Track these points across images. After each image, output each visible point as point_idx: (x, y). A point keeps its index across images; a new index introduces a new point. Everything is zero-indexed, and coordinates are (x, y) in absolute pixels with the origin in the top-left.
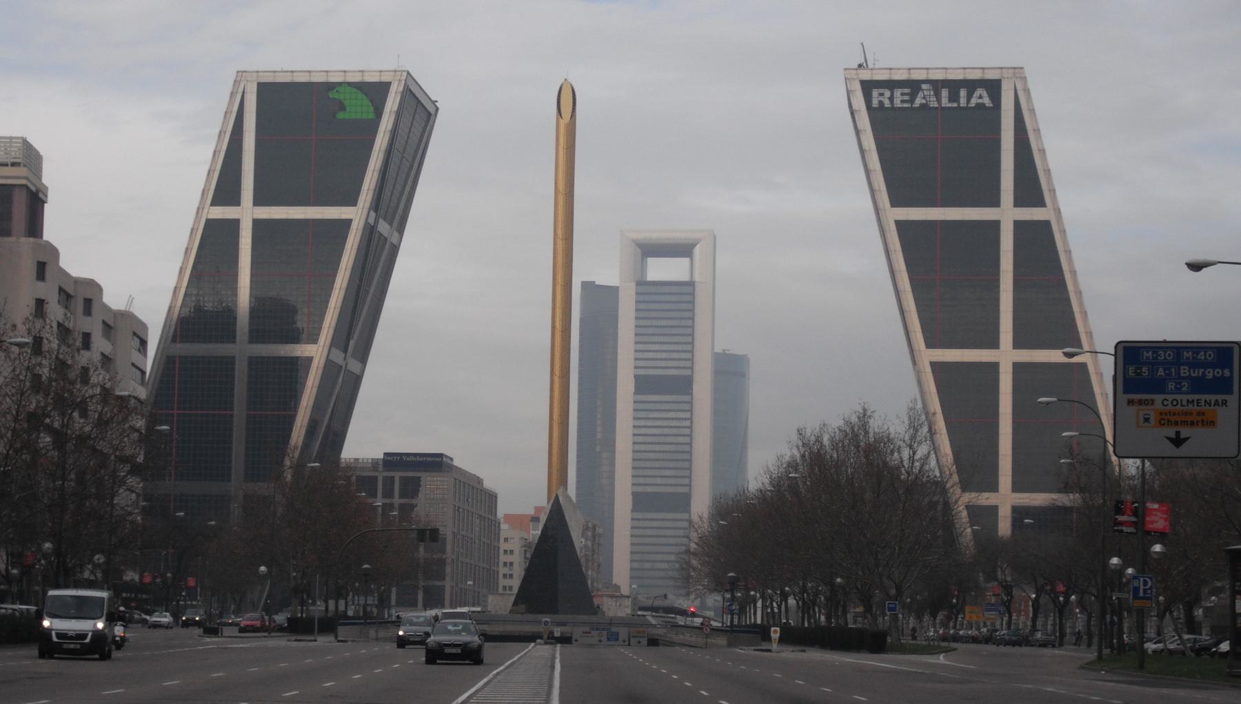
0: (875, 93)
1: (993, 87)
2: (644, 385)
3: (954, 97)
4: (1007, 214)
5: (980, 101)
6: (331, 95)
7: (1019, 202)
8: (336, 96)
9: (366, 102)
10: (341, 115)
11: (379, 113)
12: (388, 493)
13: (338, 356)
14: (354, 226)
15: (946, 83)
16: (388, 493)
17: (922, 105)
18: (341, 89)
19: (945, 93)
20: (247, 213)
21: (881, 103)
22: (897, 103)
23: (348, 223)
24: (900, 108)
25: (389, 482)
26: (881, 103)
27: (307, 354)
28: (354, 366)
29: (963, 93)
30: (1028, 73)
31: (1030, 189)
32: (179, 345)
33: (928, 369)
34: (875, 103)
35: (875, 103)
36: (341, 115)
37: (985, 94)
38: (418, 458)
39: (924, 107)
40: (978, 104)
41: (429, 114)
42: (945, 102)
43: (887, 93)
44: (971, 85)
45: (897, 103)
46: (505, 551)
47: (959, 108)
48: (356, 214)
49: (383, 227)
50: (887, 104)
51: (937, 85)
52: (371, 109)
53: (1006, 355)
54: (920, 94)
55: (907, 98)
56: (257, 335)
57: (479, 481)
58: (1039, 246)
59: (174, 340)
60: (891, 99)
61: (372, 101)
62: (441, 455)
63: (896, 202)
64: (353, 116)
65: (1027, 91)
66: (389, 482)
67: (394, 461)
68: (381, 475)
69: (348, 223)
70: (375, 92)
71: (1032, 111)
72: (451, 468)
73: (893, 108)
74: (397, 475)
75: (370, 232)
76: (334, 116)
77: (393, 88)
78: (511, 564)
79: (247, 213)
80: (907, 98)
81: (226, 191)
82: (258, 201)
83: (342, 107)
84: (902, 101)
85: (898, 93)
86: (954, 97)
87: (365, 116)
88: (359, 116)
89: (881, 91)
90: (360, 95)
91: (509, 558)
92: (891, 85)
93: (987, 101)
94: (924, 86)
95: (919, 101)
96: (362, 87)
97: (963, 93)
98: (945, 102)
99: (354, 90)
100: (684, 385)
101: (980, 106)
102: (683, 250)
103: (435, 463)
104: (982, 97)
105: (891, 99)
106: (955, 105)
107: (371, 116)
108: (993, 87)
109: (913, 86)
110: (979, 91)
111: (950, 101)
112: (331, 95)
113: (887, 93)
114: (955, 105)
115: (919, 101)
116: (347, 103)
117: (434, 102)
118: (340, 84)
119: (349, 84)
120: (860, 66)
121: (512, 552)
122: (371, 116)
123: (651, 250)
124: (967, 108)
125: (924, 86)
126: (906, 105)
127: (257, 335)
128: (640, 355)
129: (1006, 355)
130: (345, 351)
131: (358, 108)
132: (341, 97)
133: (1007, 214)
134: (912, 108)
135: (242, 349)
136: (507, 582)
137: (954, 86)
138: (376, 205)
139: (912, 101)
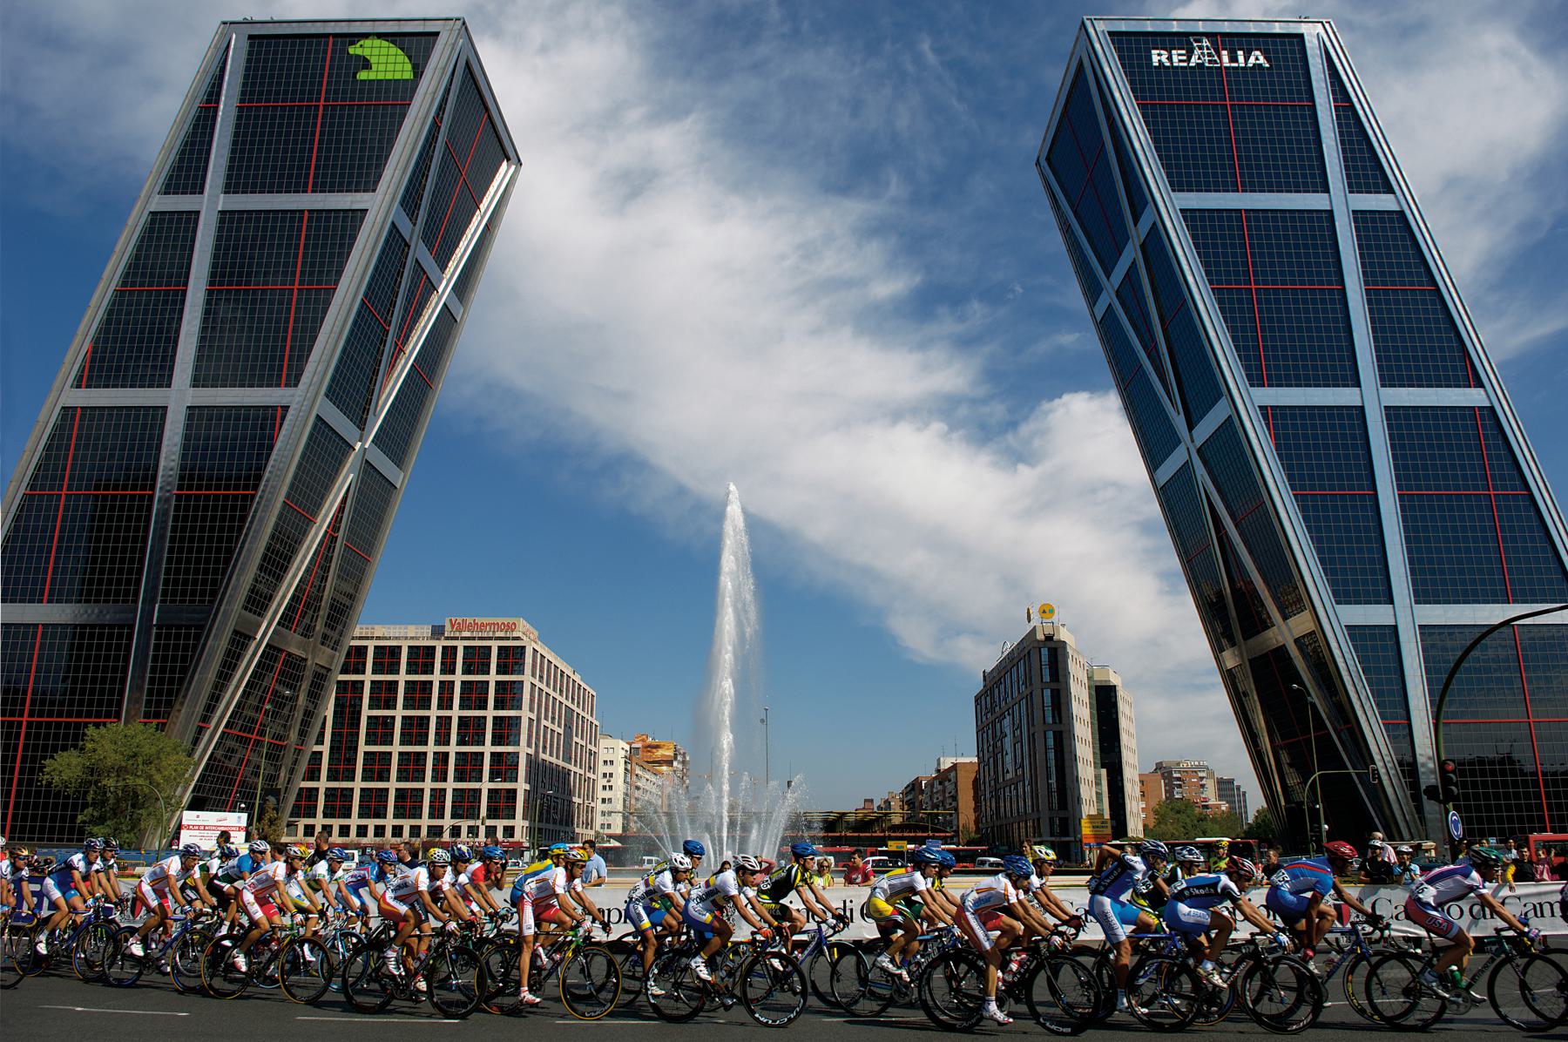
6: (351, 51)
8: (359, 52)
10: (363, 75)
11: (418, 71)
12: (449, 668)
14: (369, 218)
16: (449, 668)
18: (368, 43)
20: (212, 202)
23: (356, 217)
25: (449, 652)
31: (1368, 168)
32: (83, 392)
36: (363, 75)
49: (420, 252)
52: (409, 67)
61: (410, 58)
63: (1177, 185)
64: (381, 76)
66: (449, 652)
68: (439, 645)
69: (356, 217)
75: (395, 244)
81: (186, 172)
83: (366, 65)
87: (398, 76)
88: (389, 76)
90: (394, 50)
91: (608, 769)
95: (1194, 61)
99: (385, 44)
107: (408, 75)
112: (351, 51)
115: (1194, 61)
116: (373, 60)
118: (366, 36)
119: (380, 36)
122: (408, 75)
129: (1374, 397)
130: (361, 424)
131: (387, 64)
132: (366, 53)
133: (1341, 201)
136: (607, 794)
138: (410, 200)
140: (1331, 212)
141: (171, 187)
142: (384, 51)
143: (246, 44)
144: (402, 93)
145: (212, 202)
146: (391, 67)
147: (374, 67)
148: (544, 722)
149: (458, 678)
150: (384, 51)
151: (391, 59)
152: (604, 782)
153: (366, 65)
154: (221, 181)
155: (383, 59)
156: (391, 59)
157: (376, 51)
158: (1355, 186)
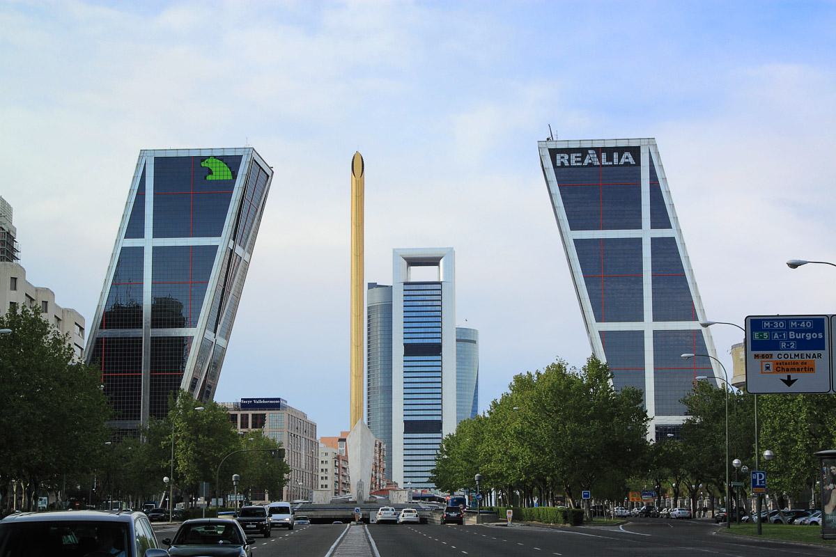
0: (558, 156)
1: (635, 151)
2: (410, 350)
3: (610, 158)
4: (646, 233)
5: (627, 160)
6: (203, 165)
7: (654, 226)
8: (206, 165)
9: (226, 168)
10: (209, 178)
11: (235, 175)
12: (244, 425)
13: (210, 335)
15: (604, 149)
16: (244, 425)
17: (589, 163)
18: (210, 160)
19: (604, 156)
20: (148, 242)
21: (562, 162)
22: (573, 163)
24: (574, 166)
25: (245, 418)
26: (562, 162)
27: (189, 335)
28: (221, 341)
29: (616, 155)
30: (658, 142)
31: (661, 217)
32: (105, 331)
33: (598, 336)
34: (559, 164)
35: (559, 164)
36: (209, 178)
37: (630, 156)
38: (264, 402)
39: (590, 165)
40: (625, 162)
41: (268, 176)
42: (604, 162)
43: (566, 157)
44: (621, 150)
45: (573, 163)
46: (322, 462)
47: (613, 165)
48: (222, 242)
50: (566, 164)
51: (599, 151)
53: (648, 326)
54: (588, 157)
55: (579, 159)
56: (156, 323)
57: (305, 416)
58: (667, 252)
59: (101, 327)
60: (569, 160)
61: (230, 168)
62: (279, 399)
63: (573, 227)
64: (218, 178)
65: (658, 154)
66: (245, 418)
67: (248, 404)
68: (239, 414)
70: (232, 162)
71: (661, 166)
72: (285, 407)
73: (570, 166)
74: (250, 413)
76: (205, 177)
77: (243, 160)
78: (326, 470)
79: (148, 242)
80: (579, 159)
81: (134, 227)
83: (210, 172)
84: (576, 162)
85: (573, 156)
86: (610, 158)
87: (225, 178)
88: (221, 178)
89: (562, 155)
90: (222, 164)
92: (569, 151)
93: (631, 161)
94: (590, 152)
95: (586, 162)
96: (222, 158)
97: (616, 155)
98: (604, 162)
99: (218, 161)
100: (436, 349)
101: (627, 164)
102: (433, 262)
103: (274, 404)
104: (628, 158)
105: (569, 160)
106: (611, 163)
107: (230, 177)
108: (635, 151)
109: (583, 152)
110: (626, 154)
111: (607, 161)
113: (566, 157)
114: (611, 163)
115: (586, 162)
116: (213, 170)
117: (271, 168)
118: (209, 157)
119: (215, 157)
120: (548, 139)
121: (326, 462)
123: (413, 262)
124: (618, 165)
125: (590, 152)
126: (578, 164)
127: (156, 323)
128: (407, 330)
129: (648, 326)
130: (215, 332)
131: (220, 173)
132: (210, 166)
133: (646, 233)
134: (582, 166)
135: (147, 332)
136: (324, 482)
137: (609, 151)
139: (582, 161)
140: (640, 239)
142: (218, 165)
144: (229, 185)
146: (221, 173)
147: (214, 173)
148: (293, 450)
150: (218, 165)
151: (221, 169)
152: (323, 474)
153: (210, 172)
155: (218, 169)
156: (221, 169)
157: (214, 165)
158: (654, 226)
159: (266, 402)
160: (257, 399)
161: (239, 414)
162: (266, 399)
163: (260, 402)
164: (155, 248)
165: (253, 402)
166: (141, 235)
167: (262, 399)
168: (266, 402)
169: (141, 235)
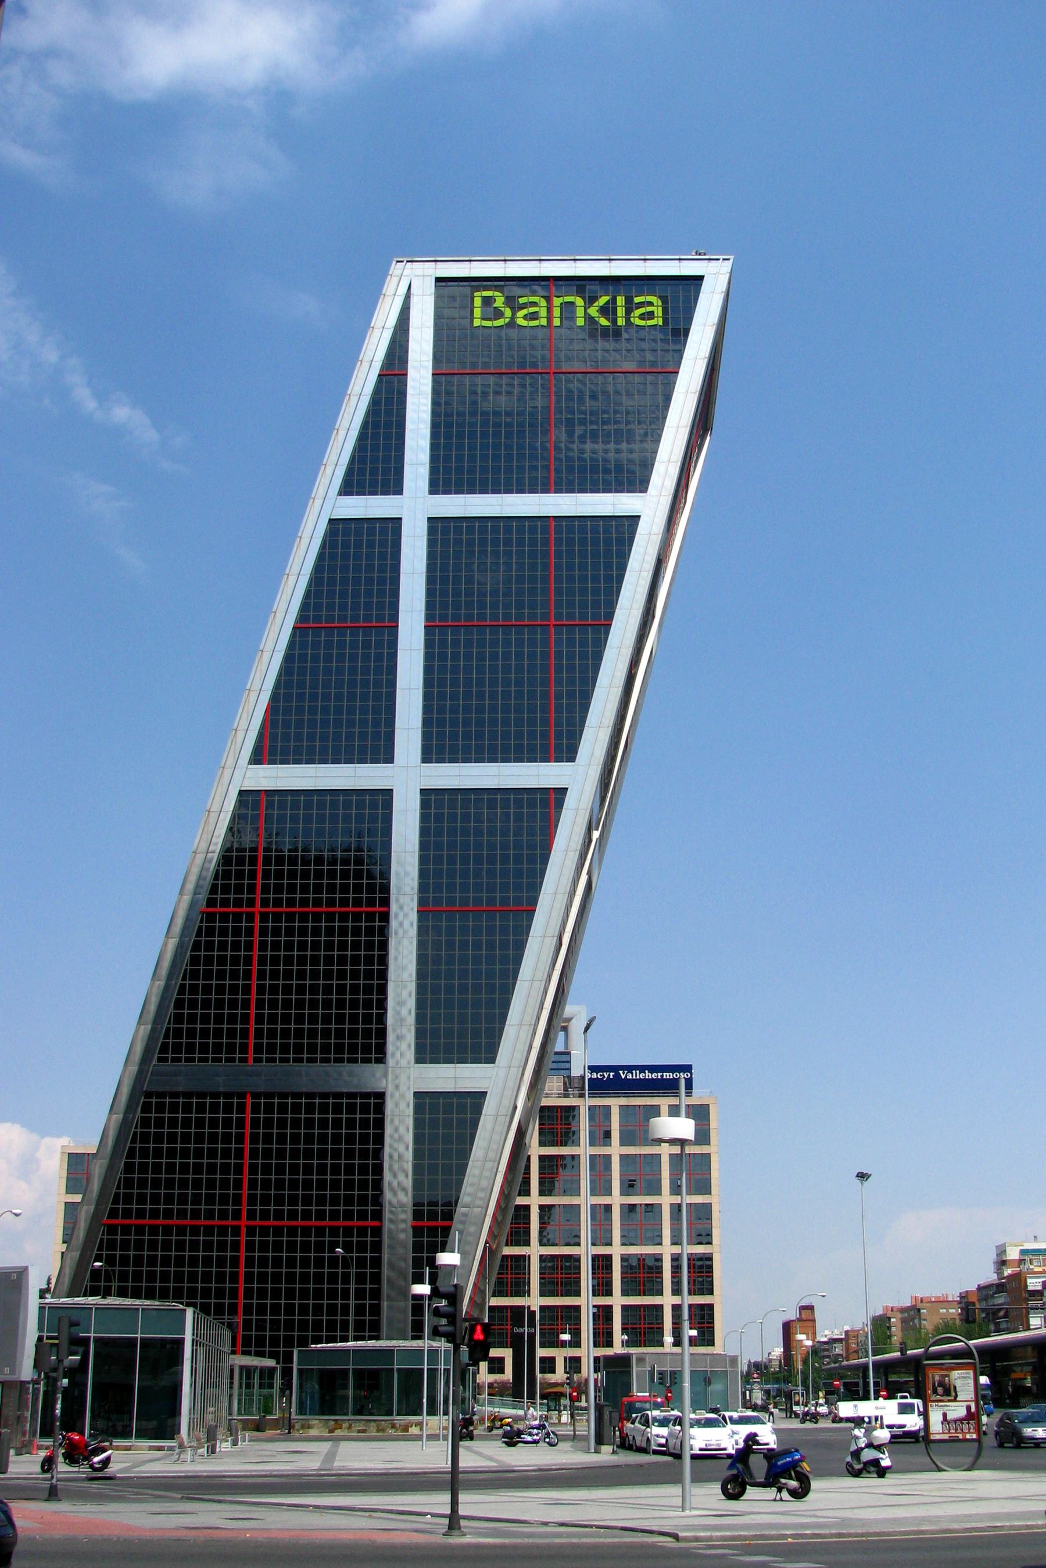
20: (416, 505)
25: (600, 1115)
38: (648, 1075)
74: (615, 1103)
81: (375, 464)
82: (438, 485)
141: (354, 483)
143: (430, 286)
145: (416, 505)
149: (615, 1150)
154: (424, 472)
159: (654, 1076)
160: (630, 1069)
161: (585, 1104)
162: (653, 1069)
163: (638, 1075)
164: (436, 524)
165: (617, 1075)
166: (393, 485)
167: (642, 1069)
168: (654, 1076)
169: (391, 482)
